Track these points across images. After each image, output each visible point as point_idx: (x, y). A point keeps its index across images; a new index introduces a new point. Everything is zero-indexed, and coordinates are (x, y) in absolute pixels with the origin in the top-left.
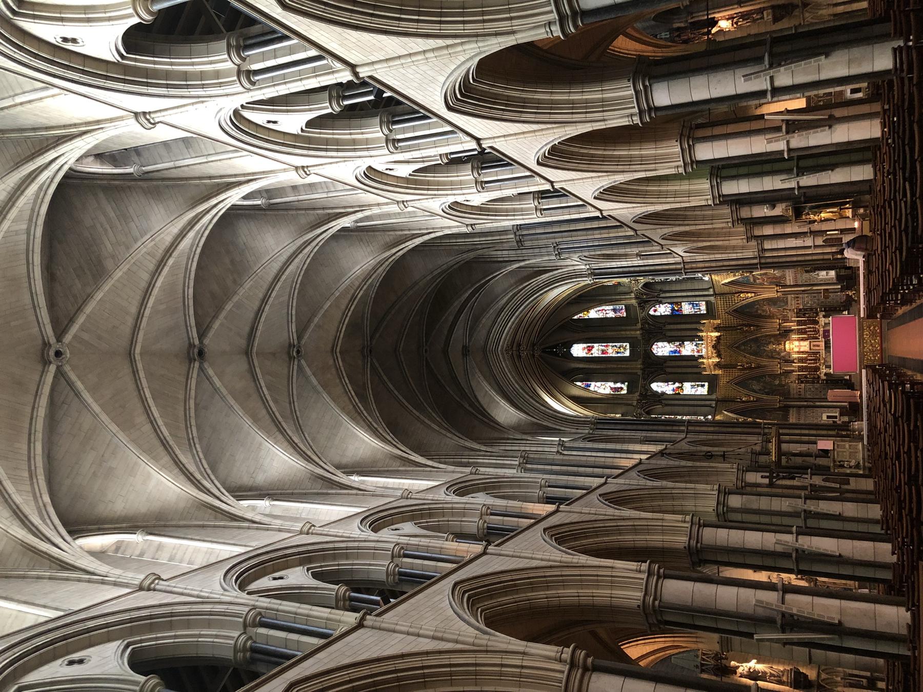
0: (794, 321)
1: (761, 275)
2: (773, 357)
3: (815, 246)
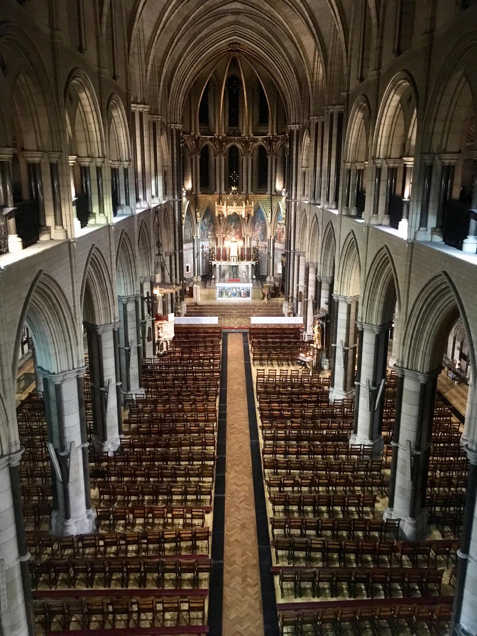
0: (250, 245)
1: (283, 229)
3: (298, 287)
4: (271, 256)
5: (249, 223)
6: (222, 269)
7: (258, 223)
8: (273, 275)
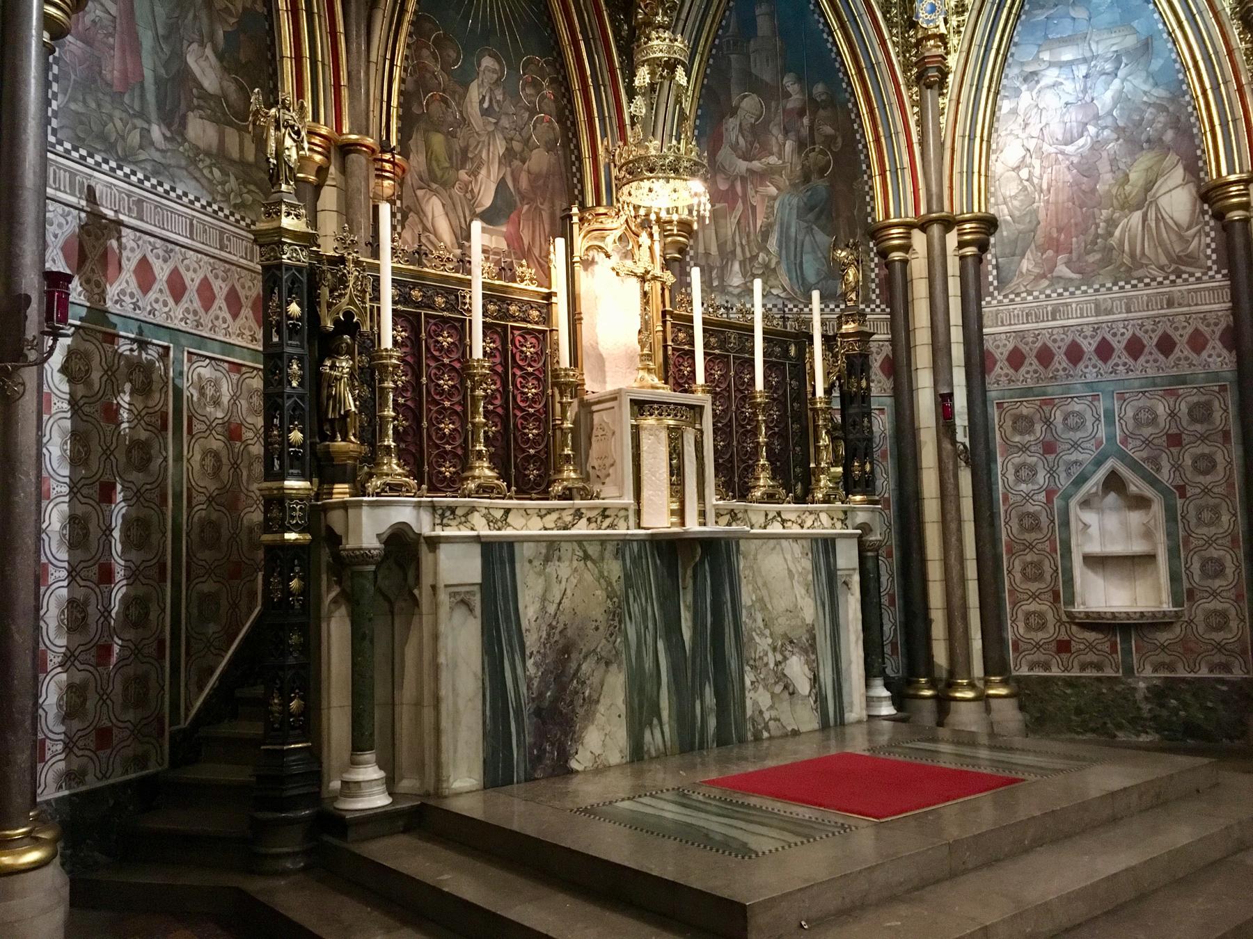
6: (529, 609)
7: (750, 104)
8: (996, 664)
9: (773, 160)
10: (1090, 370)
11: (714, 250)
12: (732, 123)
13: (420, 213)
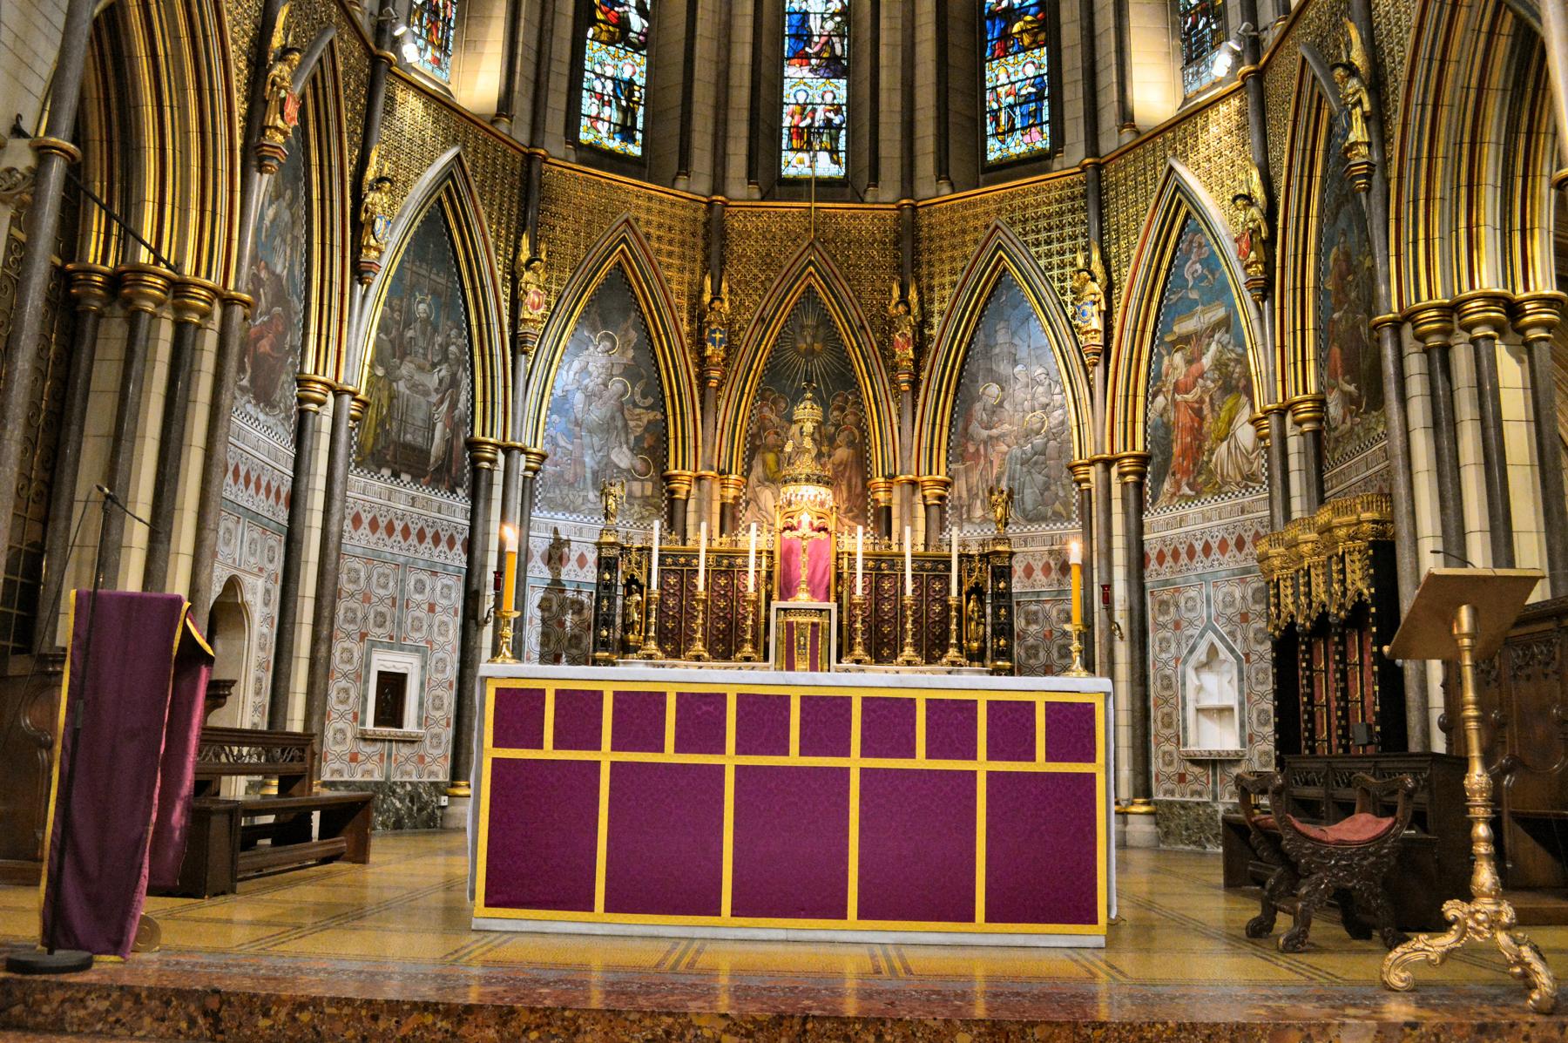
2: (753, 451)
4: (1120, 617)
5: (927, 395)
8: (1143, 789)
9: (1006, 426)
10: (1200, 565)
11: (964, 494)
12: (978, 406)
13: (755, 499)
